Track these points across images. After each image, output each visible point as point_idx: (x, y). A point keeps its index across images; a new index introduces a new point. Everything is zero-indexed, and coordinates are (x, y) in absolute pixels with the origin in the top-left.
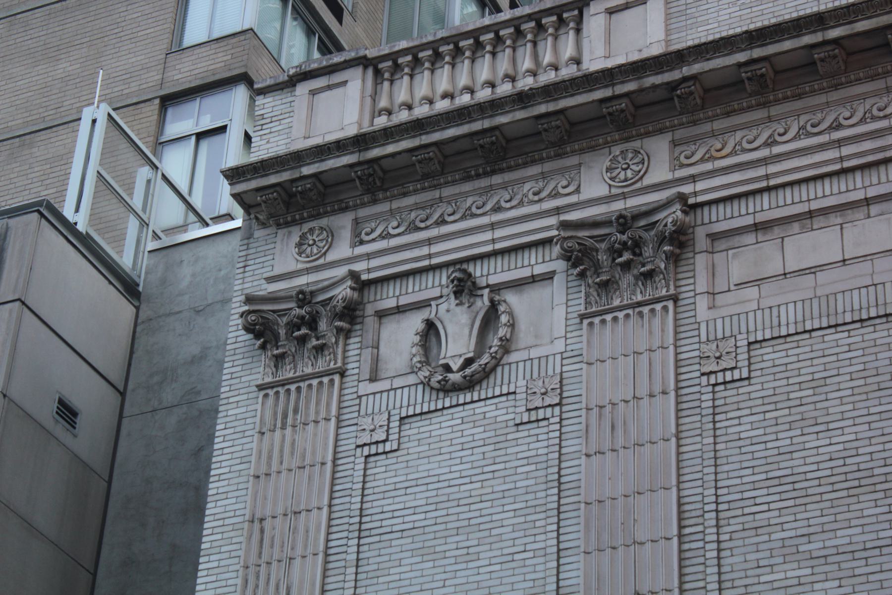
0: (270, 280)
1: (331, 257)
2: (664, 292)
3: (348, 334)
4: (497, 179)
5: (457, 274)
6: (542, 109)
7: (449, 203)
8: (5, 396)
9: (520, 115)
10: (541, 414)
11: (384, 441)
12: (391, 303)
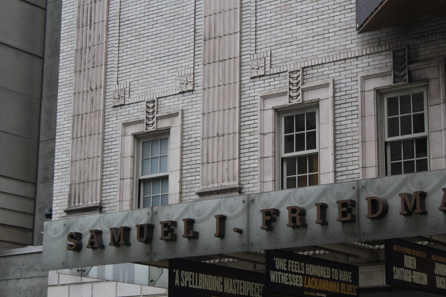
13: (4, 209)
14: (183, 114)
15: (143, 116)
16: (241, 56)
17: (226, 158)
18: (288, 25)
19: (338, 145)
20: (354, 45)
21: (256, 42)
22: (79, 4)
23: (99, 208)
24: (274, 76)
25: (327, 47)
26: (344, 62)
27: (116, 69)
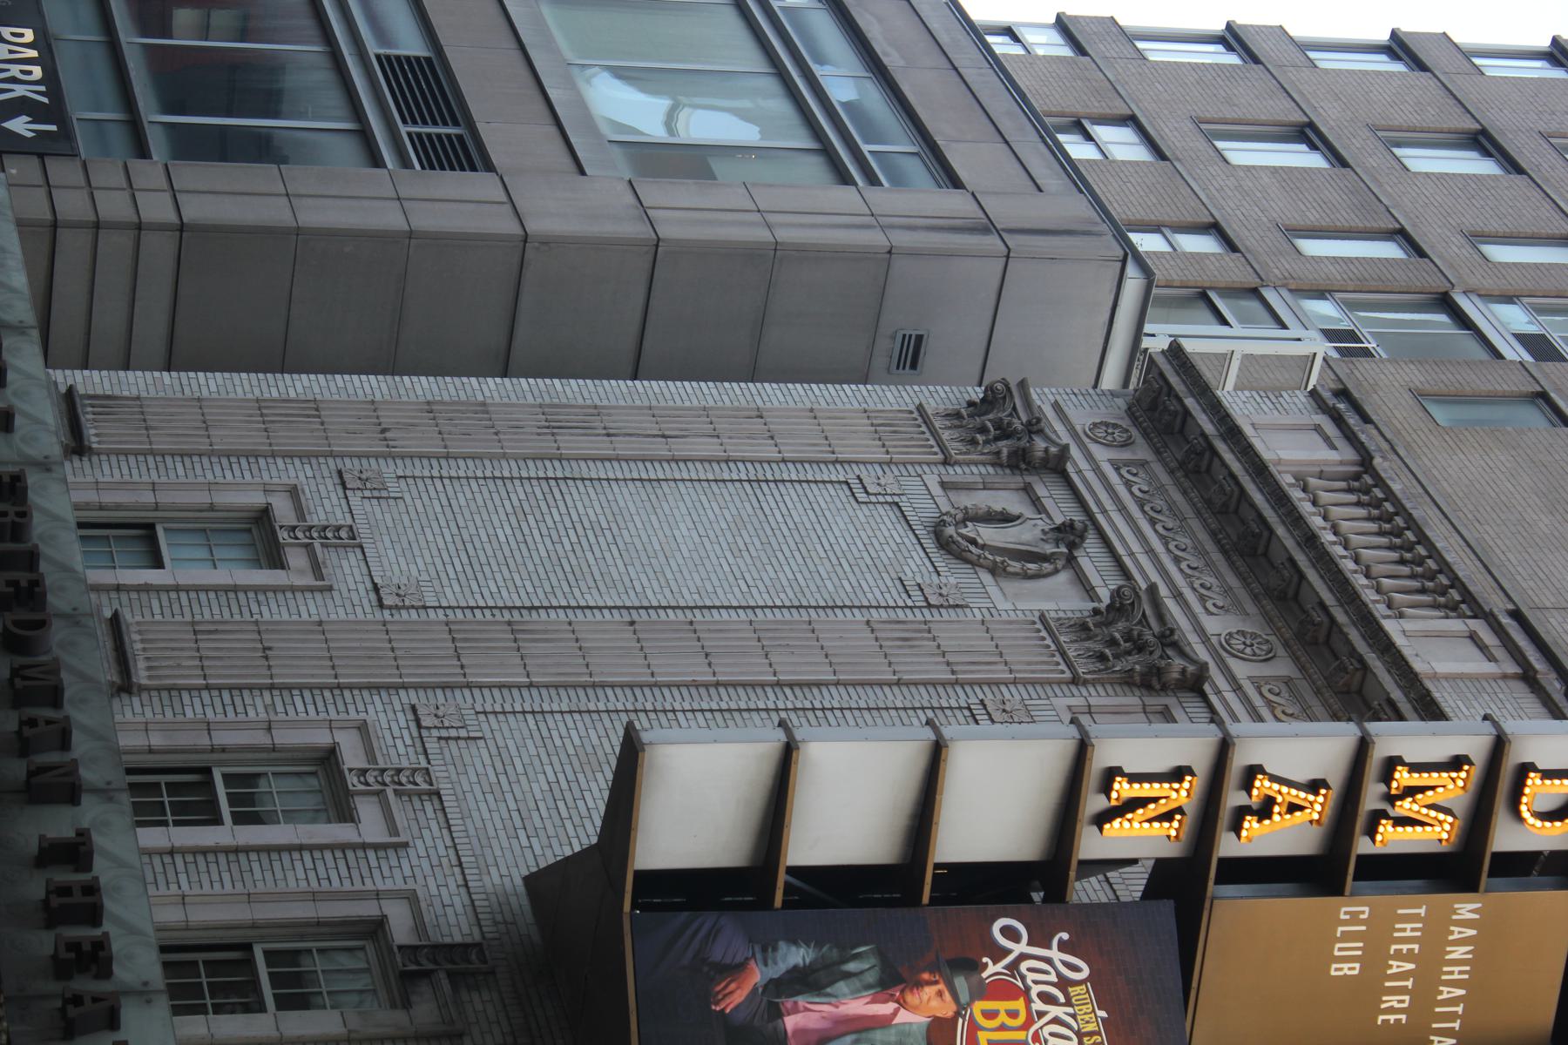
0: (1056, 407)
1: (1094, 449)
2: (1080, 671)
3: (993, 465)
4: (1217, 556)
5: (1078, 526)
6: (1301, 559)
7: (1181, 527)
8: (890, 252)
9: (1290, 543)
10: (916, 593)
11: (867, 492)
12: (1041, 491)
13: (88, 333)
14: (321, 590)
15: (317, 518)
16: (469, 686)
17: (206, 663)
18: (548, 769)
19: (242, 857)
20: (497, 880)
21: (504, 713)
22: (604, 407)
23: (78, 446)
24: (418, 744)
25: (492, 833)
26: (455, 862)
27: (435, 473)
